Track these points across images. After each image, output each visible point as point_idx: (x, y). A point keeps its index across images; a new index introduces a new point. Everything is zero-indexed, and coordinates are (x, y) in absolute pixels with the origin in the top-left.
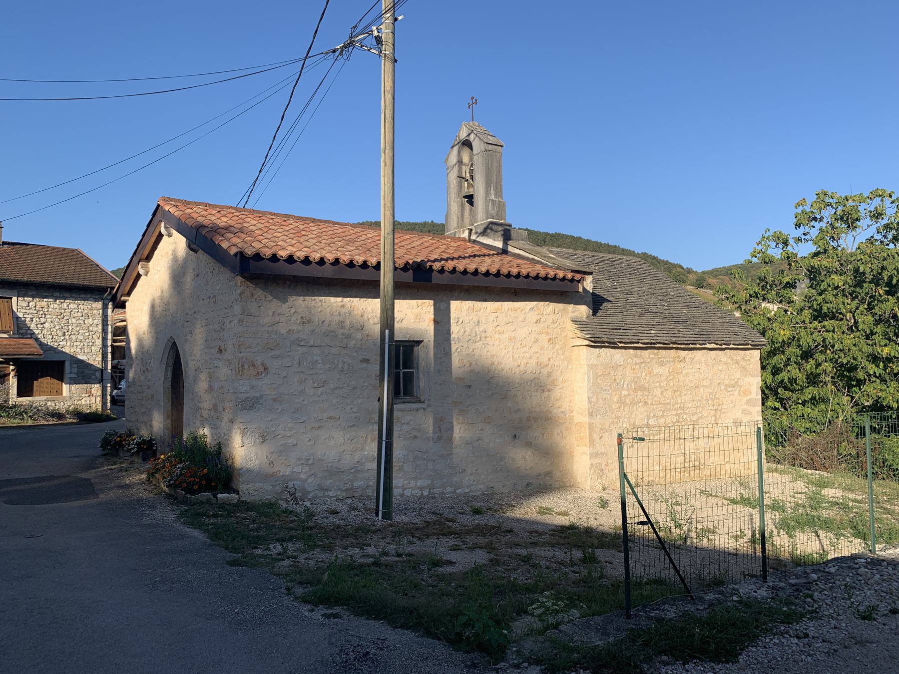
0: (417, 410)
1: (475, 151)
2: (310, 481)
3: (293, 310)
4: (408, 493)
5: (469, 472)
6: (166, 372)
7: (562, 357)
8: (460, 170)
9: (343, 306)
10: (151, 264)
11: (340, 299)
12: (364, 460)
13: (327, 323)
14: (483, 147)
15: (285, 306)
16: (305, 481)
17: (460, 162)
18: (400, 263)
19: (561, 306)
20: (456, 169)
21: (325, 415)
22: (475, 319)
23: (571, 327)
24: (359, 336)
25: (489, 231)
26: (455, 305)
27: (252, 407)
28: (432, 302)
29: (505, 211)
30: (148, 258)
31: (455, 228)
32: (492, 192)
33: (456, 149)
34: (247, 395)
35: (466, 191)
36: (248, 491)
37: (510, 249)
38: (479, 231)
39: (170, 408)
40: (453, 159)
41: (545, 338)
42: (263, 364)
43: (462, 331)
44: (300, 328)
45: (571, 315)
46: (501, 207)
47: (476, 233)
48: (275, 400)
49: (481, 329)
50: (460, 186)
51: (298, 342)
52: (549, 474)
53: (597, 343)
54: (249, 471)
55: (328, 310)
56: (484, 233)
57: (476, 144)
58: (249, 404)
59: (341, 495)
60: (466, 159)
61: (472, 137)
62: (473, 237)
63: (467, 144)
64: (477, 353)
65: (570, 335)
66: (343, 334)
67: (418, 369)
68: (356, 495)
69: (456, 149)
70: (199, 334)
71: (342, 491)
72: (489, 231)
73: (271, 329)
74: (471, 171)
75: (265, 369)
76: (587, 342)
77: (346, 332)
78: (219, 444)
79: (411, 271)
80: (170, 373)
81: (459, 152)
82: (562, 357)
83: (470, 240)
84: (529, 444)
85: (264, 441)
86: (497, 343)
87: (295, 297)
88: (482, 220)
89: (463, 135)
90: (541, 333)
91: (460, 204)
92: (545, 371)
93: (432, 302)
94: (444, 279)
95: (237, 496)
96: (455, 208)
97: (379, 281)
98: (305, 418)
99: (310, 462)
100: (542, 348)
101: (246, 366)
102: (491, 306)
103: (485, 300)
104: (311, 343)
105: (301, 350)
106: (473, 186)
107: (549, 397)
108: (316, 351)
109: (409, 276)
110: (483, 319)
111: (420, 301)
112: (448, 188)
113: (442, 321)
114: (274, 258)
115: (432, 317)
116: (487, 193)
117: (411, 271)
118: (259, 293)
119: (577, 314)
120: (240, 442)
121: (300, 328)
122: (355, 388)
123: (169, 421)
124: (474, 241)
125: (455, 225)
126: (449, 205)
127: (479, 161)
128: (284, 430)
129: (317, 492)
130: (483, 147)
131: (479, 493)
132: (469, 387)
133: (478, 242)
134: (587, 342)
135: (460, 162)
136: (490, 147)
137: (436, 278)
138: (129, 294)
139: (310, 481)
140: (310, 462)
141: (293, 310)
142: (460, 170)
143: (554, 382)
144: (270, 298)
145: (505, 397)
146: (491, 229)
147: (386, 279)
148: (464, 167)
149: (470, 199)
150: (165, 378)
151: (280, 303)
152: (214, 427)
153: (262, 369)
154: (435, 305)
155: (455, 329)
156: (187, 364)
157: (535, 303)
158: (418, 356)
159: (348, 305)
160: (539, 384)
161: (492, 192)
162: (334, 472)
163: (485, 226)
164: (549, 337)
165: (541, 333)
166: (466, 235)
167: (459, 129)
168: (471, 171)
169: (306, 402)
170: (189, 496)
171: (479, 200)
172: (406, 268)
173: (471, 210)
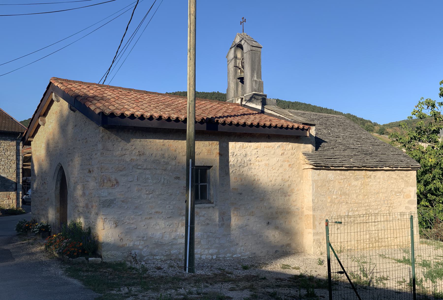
0: (209, 208)
1: (245, 50)
2: (145, 250)
3: (133, 147)
4: (204, 257)
5: (241, 244)
6: (57, 184)
7: (297, 176)
8: (236, 62)
9: (164, 145)
11: (162, 141)
12: (177, 238)
13: (154, 155)
14: (250, 48)
16: (141, 250)
17: (236, 57)
18: (199, 118)
19: (296, 145)
20: (233, 62)
21: (153, 211)
22: (244, 153)
23: (302, 157)
24: (173, 163)
25: (253, 99)
26: (232, 145)
27: (109, 206)
28: (218, 142)
29: (263, 87)
31: (233, 98)
32: (255, 75)
33: (233, 49)
34: (106, 198)
35: (239, 74)
36: (107, 256)
37: (266, 110)
38: (247, 99)
39: (59, 206)
40: (231, 55)
41: (287, 164)
42: (116, 180)
43: (236, 160)
44: (138, 158)
45: (303, 150)
46: (261, 85)
47: (245, 100)
48: (123, 201)
49: (248, 159)
50: (236, 72)
51: (137, 166)
53: (318, 167)
54: (108, 244)
55: (155, 147)
56: (250, 100)
58: (107, 204)
59: (163, 258)
60: (239, 55)
61: (243, 42)
62: (244, 103)
63: (240, 46)
64: (245, 173)
65: (302, 162)
67: (209, 183)
68: (172, 258)
69: (233, 49)
70: (77, 161)
71: (164, 256)
72: (253, 99)
73: (120, 158)
74: (242, 63)
75: (117, 182)
76: (312, 167)
77: (166, 160)
78: (89, 228)
79: (205, 124)
80: (59, 185)
81: (235, 52)
82: (297, 176)
84: (277, 228)
85: (116, 226)
86: (257, 167)
87: (134, 139)
88: (249, 93)
89: (237, 41)
90: (284, 161)
92: (287, 184)
93: (218, 142)
94: (226, 129)
95: (100, 259)
96: (232, 85)
97: (186, 130)
98: (141, 213)
99: (145, 239)
100: (285, 170)
101: (106, 181)
102: (253, 145)
103: (250, 142)
104: (145, 167)
105: (139, 171)
106: (243, 72)
107: (289, 199)
108: (148, 172)
109: (204, 127)
110: (249, 153)
111: (211, 142)
113: (224, 154)
115: (218, 151)
116: (252, 76)
117: (205, 124)
119: (306, 150)
120: (102, 226)
121: (138, 158)
122: (171, 195)
123: (58, 214)
124: (244, 105)
125: (233, 96)
126: (229, 83)
127: (247, 58)
128: (129, 219)
129: (149, 257)
130: (250, 48)
131: (246, 257)
132: (241, 194)
133: (247, 106)
134: (312, 167)
135: (236, 57)
136: (254, 48)
137: (221, 128)
139: (145, 250)
140: (145, 239)
141: (133, 147)
142: (236, 62)
143: (292, 191)
145: (262, 200)
146: (255, 98)
147: (190, 128)
148: (238, 61)
149: (242, 80)
150: (56, 188)
152: (86, 218)
153: (115, 182)
154: (220, 144)
155: (232, 159)
156: (69, 180)
157: (281, 143)
158: (210, 176)
159: (167, 144)
160: (284, 192)
161: (255, 75)
162: (159, 244)
163: (251, 96)
164: (289, 163)
165: (284, 161)
166: (239, 102)
168: (242, 63)
169: (142, 203)
170: (71, 259)
171: (247, 81)
172: (203, 121)
173: (242, 87)
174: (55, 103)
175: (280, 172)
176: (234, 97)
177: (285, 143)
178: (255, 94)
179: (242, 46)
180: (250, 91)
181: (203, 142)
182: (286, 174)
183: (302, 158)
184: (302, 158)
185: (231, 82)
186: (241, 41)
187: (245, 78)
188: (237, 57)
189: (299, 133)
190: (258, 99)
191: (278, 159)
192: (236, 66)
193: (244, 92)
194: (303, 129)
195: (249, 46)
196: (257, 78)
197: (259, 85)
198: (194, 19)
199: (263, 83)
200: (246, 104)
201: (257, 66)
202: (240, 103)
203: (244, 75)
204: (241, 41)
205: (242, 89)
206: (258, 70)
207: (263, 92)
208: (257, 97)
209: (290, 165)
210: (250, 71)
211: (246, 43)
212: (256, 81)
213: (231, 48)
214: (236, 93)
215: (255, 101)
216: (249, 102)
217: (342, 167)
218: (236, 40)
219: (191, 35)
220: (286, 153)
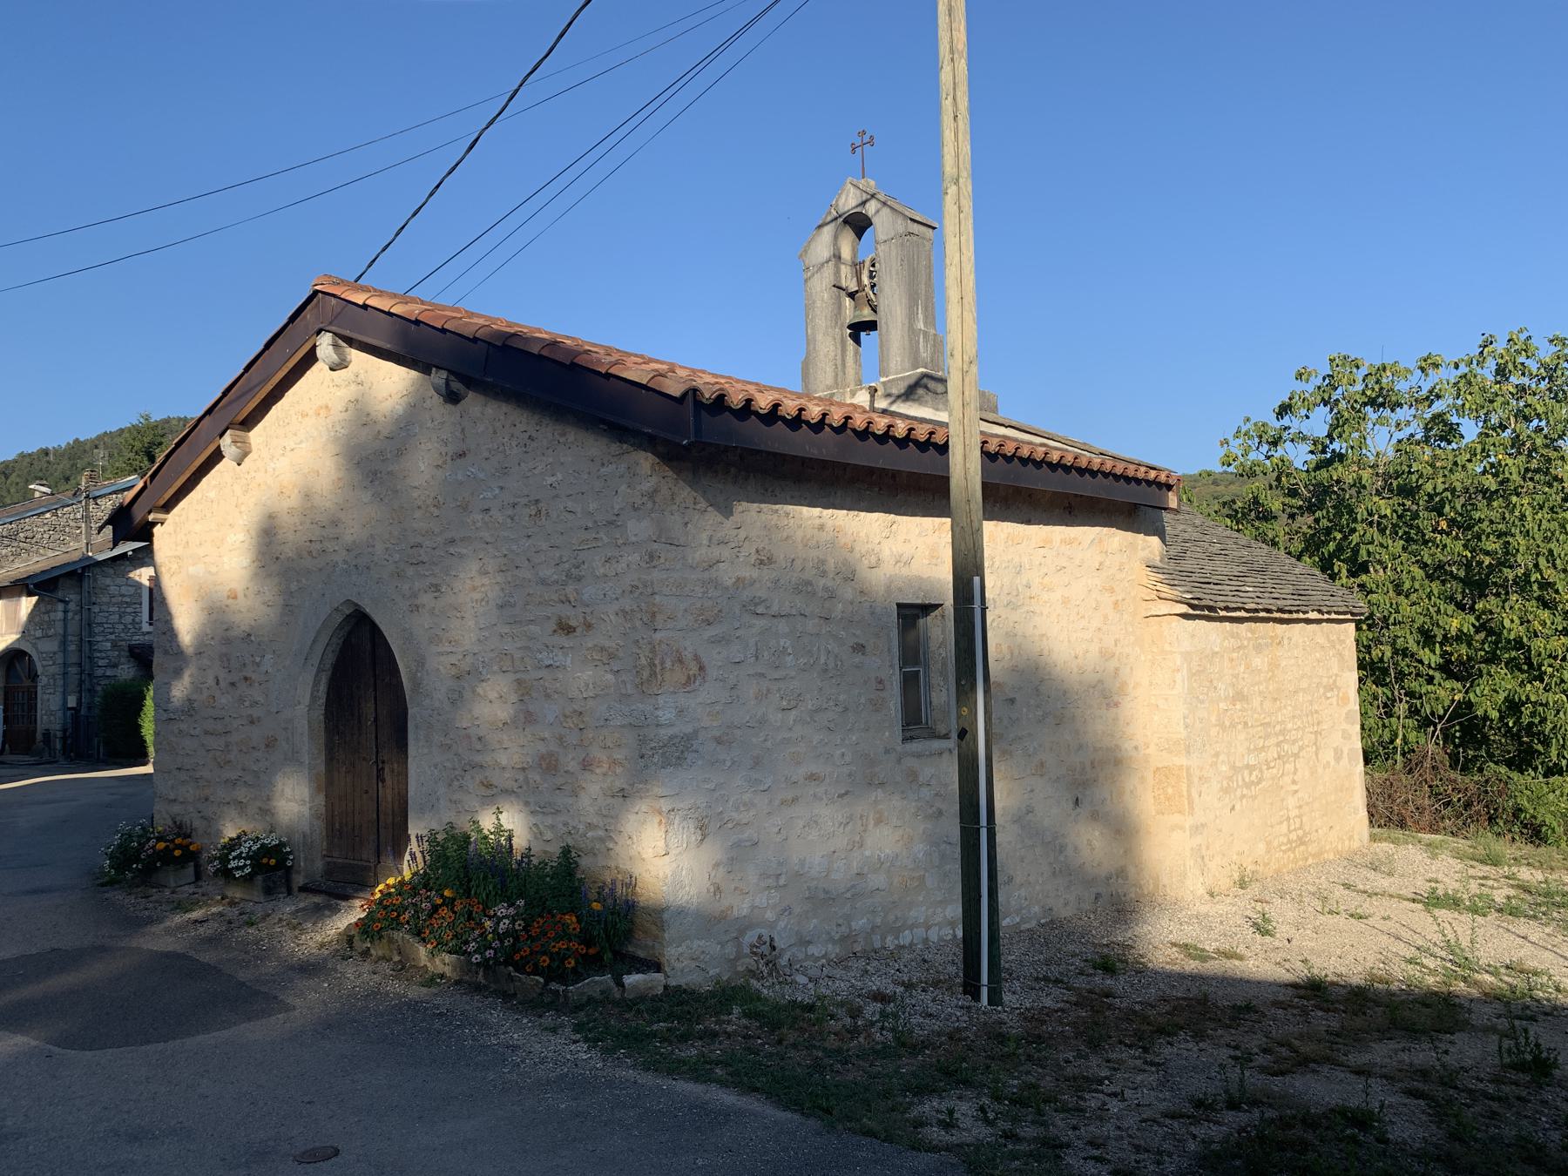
0: (941, 754)
2: (782, 924)
3: (742, 534)
4: (933, 936)
5: (1018, 880)
6: (316, 683)
9: (821, 527)
10: (256, 435)
11: (816, 511)
12: (866, 870)
13: (798, 563)
15: (729, 523)
16: (772, 925)
20: (829, 271)
21: (802, 771)
24: (848, 593)
27: (680, 761)
30: (248, 423)
31: (829, 388)
33: (828, 231)
34: (670, 732)
36: (687, 962)
38: (895, 391)
39: (323, 768)
42: (697, 658)
44: (755, 573)
45: (1142, 554)
48: (719, 741)
51: (753, 607)
52: (1121, 873)
53: (1201, 610)
54: (681, 912)
55: (799, 534)
57: (883, 223)
58: (658, 757)
59: (834, 950)
62: (881, 404)
63: (858, 224)
66: (825, 590)
67: (927, 667)
68: (858, 948)
70: (473, 588)
71: (834, 942)
72: (921, 391)
73: (706, 575)
75: (701, 668)
76: (1184, 609)
77: (830, 584)
78: (566, 851)
80: (323, 687)
81: (836, 238)
83: (873, 409)
84: (1095, 816)
85: (704, 837)
87: (745, 504)
89: (848, 201)
91: (838, 338)
92: (1112, 664)
95: (659, 976)
98: (768, 782)
99: (782, 882)
101: (668, 664)
103: (1029, 522)
104: (775, 609)
105: (761, 623)
107: (1116, 719)
108: (783, 626)
112: (808, 308)
114: (748, 407)
116: (912, 317)
118: (685, 493)
120: (661, 844)
121: (755, 573)
122: (846, 709)
123: (321, 799)
125: (830, 381)
126: (810, 341)
128: (737, 809)
129: (794, 950)
131: (1033, 924)
132: (1012, 701)
134: (1184, 609)
136: (916, 228)
138: (168, 507)
139: (782, 924)
140: (782, 882)
141: (742, 534)
142: (837, 272)
143: (1124, 684)
144: (703, 504)
145: (1059, 722)
146: (926, 387)
150: (313, 698)
151: (720, 518)
152: (538, 808)
153: (694, 670)
156: (421, 662)
158: (928, 638)
159: (830, 523)
160: (1106, 692)
162: (821, 899)
163: (912, 381)
167: (838, 189)
169: (769, 744)
170: (554, 986)
173: (856, 353)
174: (317, 375)
180: (907, 365)
181: (918, 519)
183: (1145, 581)
185: (820, 337)
186: (864, 203)
196: (925, 324)
200: (894, 408)
204: (864, 203)
208: (932, 384)
209: (1116, 603)
211: (886, 211)
212: (925, 333)
213: (820, 227)
217: (1239, 609)
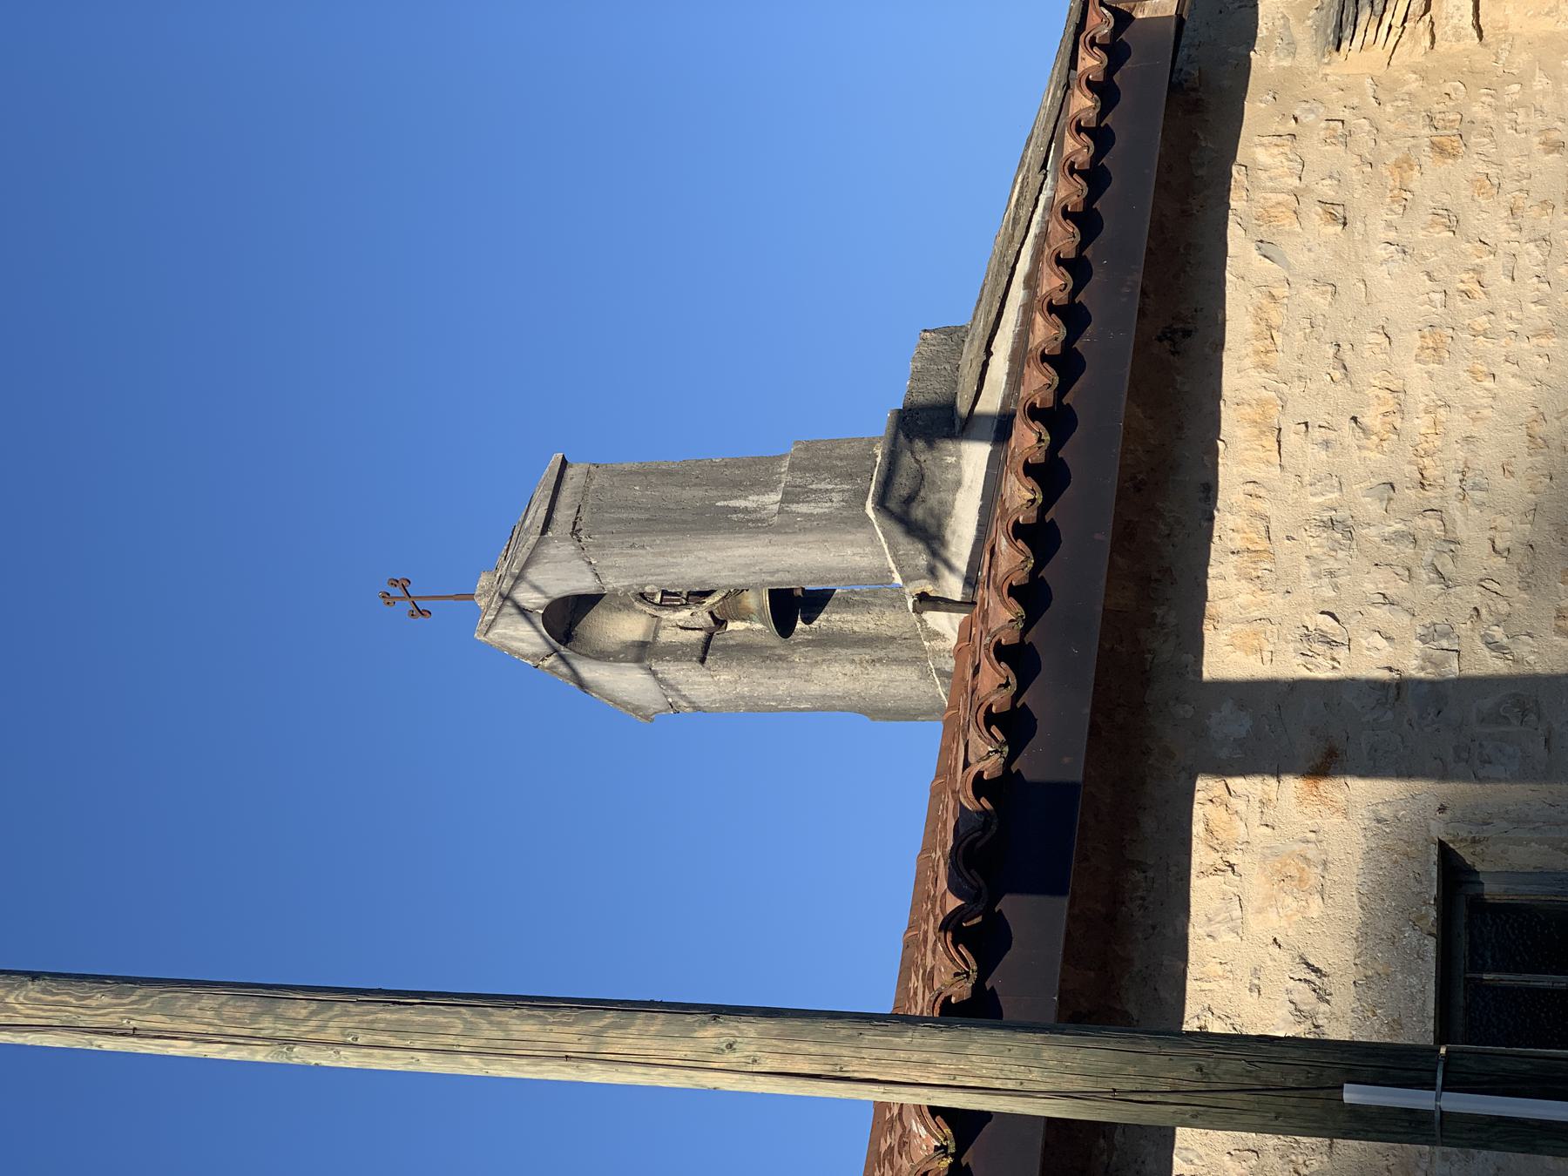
1: (584, 583)
7: (1540, 83)
8: (675, 653)
14: (560, 548)
17: (642, 652)
18: (949, 973)
19: (1256, 108)
20: (671, 671)
22: (1315, 542)
23: (1365, 55)
25: (918, 512)
26: (1228, 655)
28: (1206, 788)
29: (835, 443)
31: (925, 675)
32: (751, 502)
33: (590, 671)
35: (752, 627)
37: (990, 403)
38: (923, 560)
40: (627, 683)
41: (1430, 178)
43: (1381, 614)
45: (1306, 58)
46: (817, 461)
47: (932, 573)
49: (1374, 508)
50: (745, 651)
56: (930, 535)
57: (562, 575)
60: (628, 627)
61: (527, 597)
62: (954, 587)
63: (566, 619)
64: (1512, 531)
65: (1414, 48)
69: (590, 671)
72: (918, 512)
74: (670, 599)
79: (1008, 905)
81: (603, 656)
82: (1540, 83)
83: (967, 604)
86: (1458, 423)
88: (862, 551)
89: (525, 638)
90: (1404, 199)
91: (814, 654)
93: (1206, 788)
94: (1063, 708)
96: (836, 677)
97: (1050, 1121)
100: (1488, 185)
102: (1240, 459)
103: (1209, 490)
106: (737, 592)
109: (1038, 922)
110: (1317, 501)
111: (1201, 855)
112: (755, 708)
113: (1313, 730)
115: (1292, 785)
116: (753, 524)
117: (1008, 905)
119: (1304, 34)
124: (971, 581)
126: (826, 706)
127: (621, 568)
130: (560, 548)
133: (974, 564)
135: (642, 652)
136: (563, 515)
137: (1056, 758)
142: (675, 653)
146: (910, 500)
147: (1024, 1077)
148: (666, 636)
149: (792, 607)
154: (1223, 770)
155: (1372, 655)
157: (1234, 233)
161: (751, 502)
163: (897, 531)
164: (1427, 157)
165: (1404, 199)
166: (946, 624)
167: (503, 657)
168: (670, 599)
171: (799, 560)
172: (979, 934)
173: (847, 604)
175: (1500, 230)
176: (917, 660)
177: (1236, 201)
178: (881, 504)
179: (565, 600)
180: (861, 536)
182: (1520, 176)
183: (1379, 53)
184: (1379, 53)
185: (814, 689)
186: (524, 612)
187: (784, 580)
188: (643, 645)
189: (1145, 78)
190: (921, 477)
191: (1381, 252)
192: (704, 652)
193: (874, 592)
194: (1115, 51)
195: (551, 550)
196: (769, 487)
197: (816, 469)
198: (33, 989)
199: (808, 446)
200: (962, 564)
201: (687, 493)
202: (958, 618)
203: (756, 588)
204: (524, 612)
205: (866, 605)
206: (717, 483)
207: (872, 443)
208: (903, 485)
209: (1440, 149)
210: (719, 541)
211: (533, 574)
212: (788, 498)
213: (582, 684)
214: (893, 652)
215: (933, 500)
216: (943, 543)
218: (527, 648)
219: (157, 1021)
220: (1327, 190)
